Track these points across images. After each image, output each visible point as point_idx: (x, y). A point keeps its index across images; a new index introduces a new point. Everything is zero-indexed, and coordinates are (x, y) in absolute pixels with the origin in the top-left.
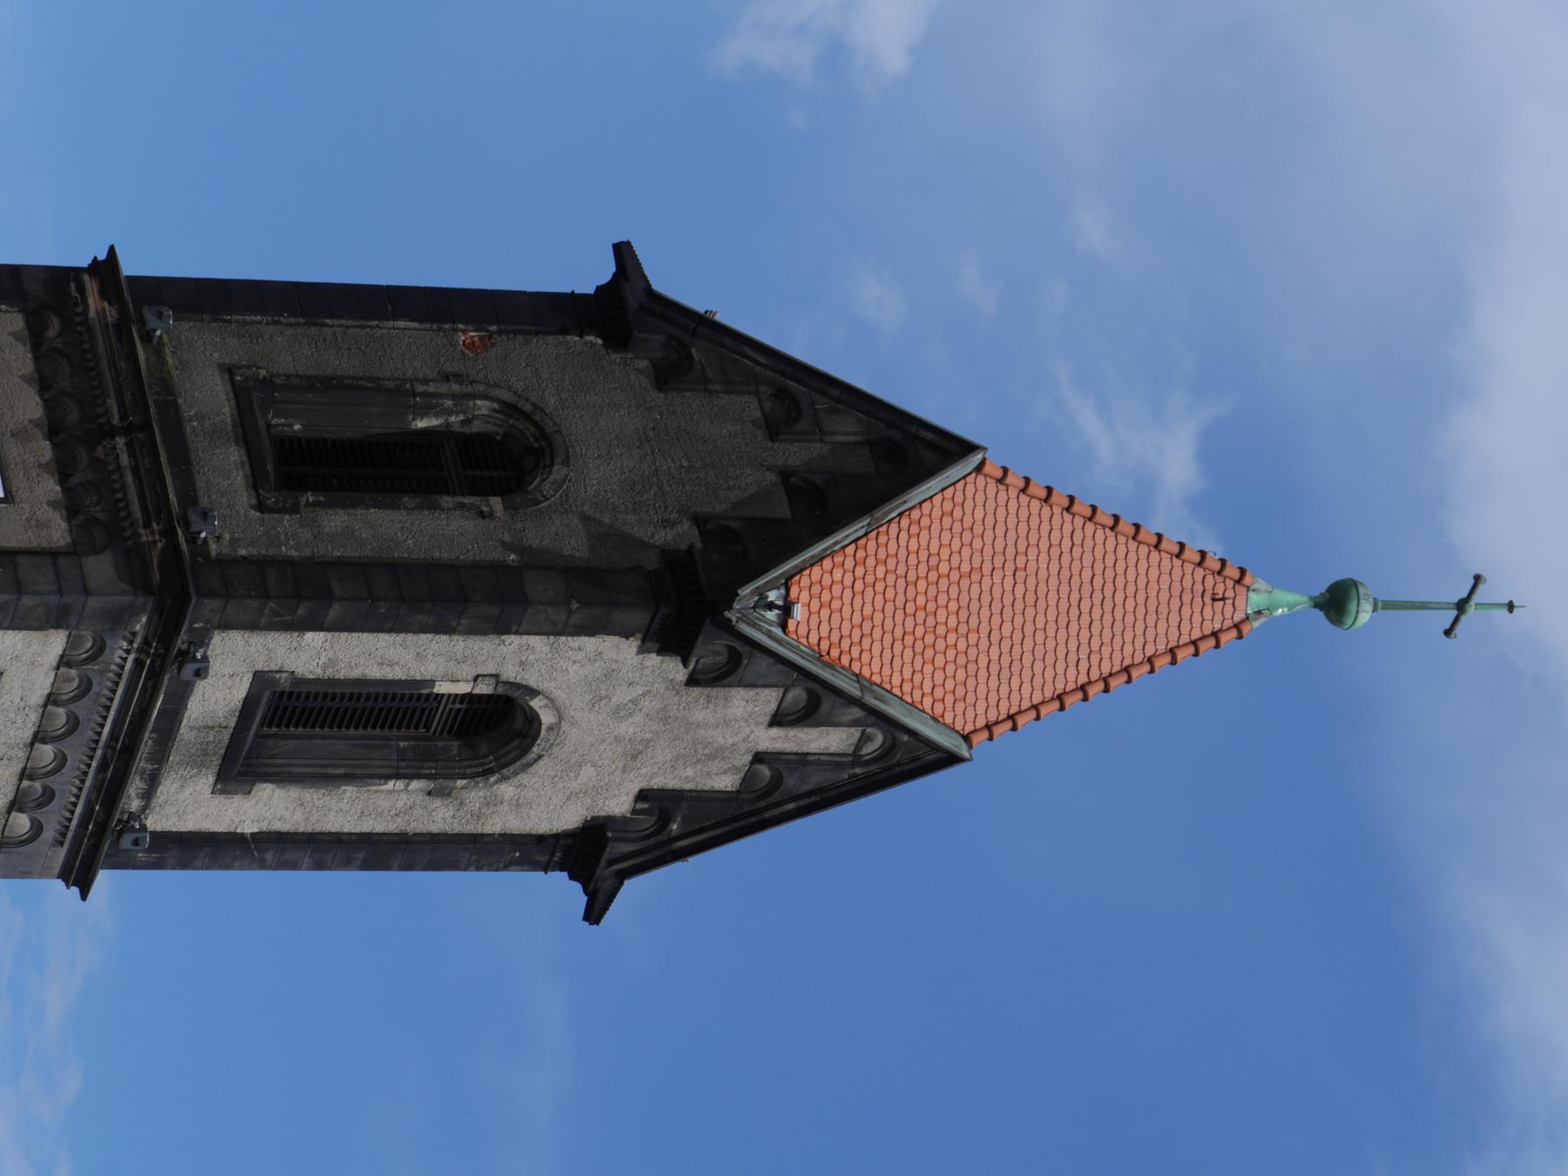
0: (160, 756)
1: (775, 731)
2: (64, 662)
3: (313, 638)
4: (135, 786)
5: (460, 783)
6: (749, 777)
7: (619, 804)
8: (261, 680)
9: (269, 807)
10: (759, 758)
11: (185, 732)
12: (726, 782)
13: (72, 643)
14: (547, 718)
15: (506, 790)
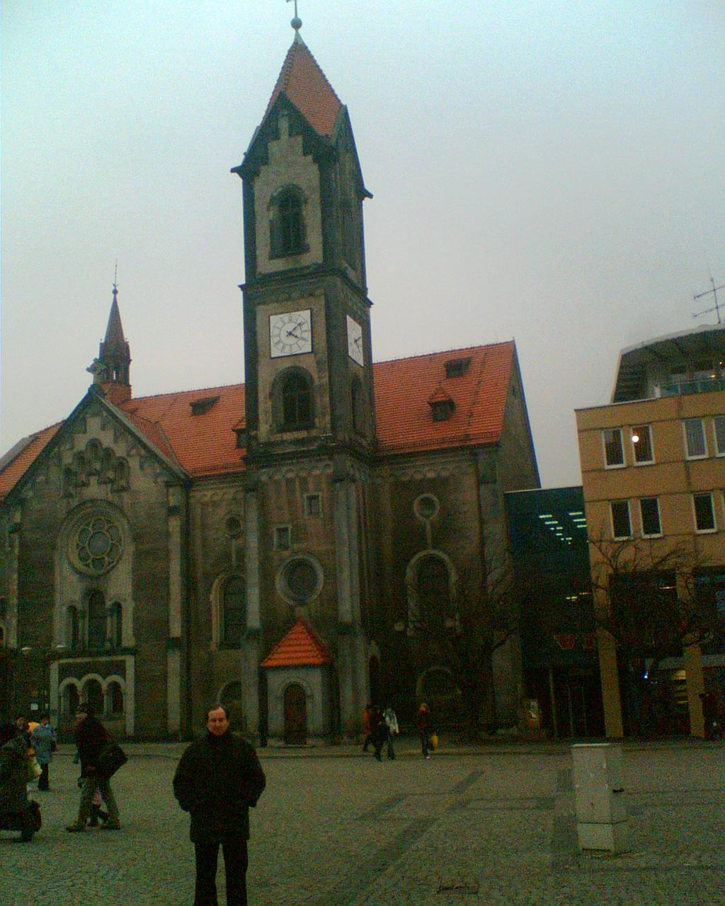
0: (295, 270)
1: (282, 137)
2: (264, 303)
3: (258, 252)
4: (307, 271)
5: (302, 198)
6: (297, 134)
7: (310, 158)
8: (271, 258)
9: (314, 239)
10: (290, 135)
11: (291, 267)
12: (300, 139)
13: (259, 304)
14: (280, 189)
15: (304, 187)
